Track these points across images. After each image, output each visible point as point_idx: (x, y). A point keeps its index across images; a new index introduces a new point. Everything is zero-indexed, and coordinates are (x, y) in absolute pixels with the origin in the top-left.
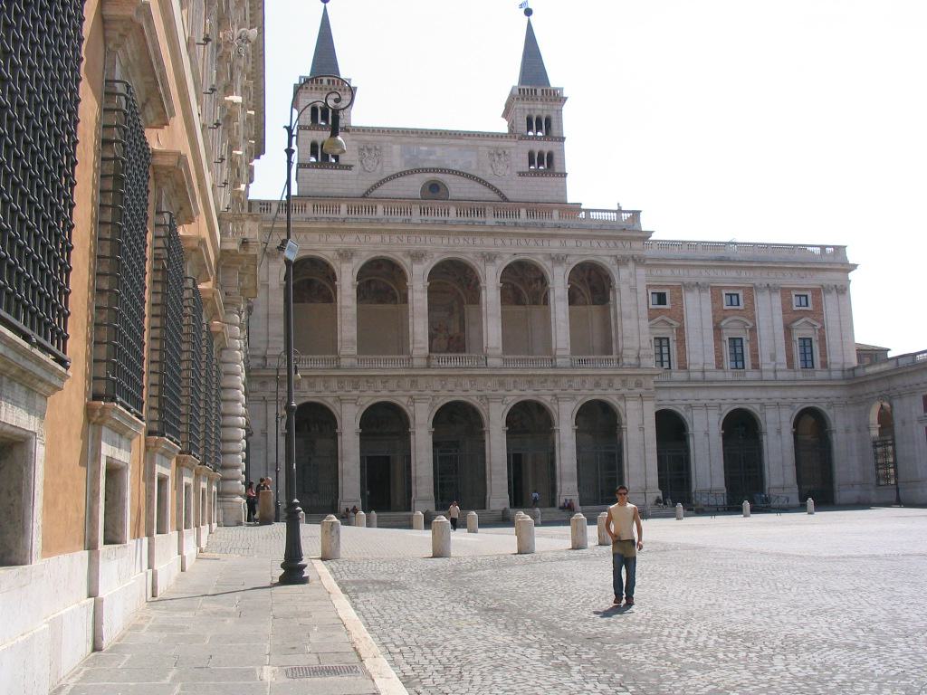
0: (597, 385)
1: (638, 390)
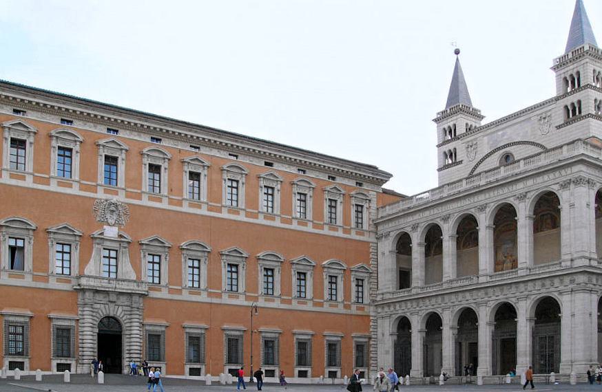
1: (571, 286)
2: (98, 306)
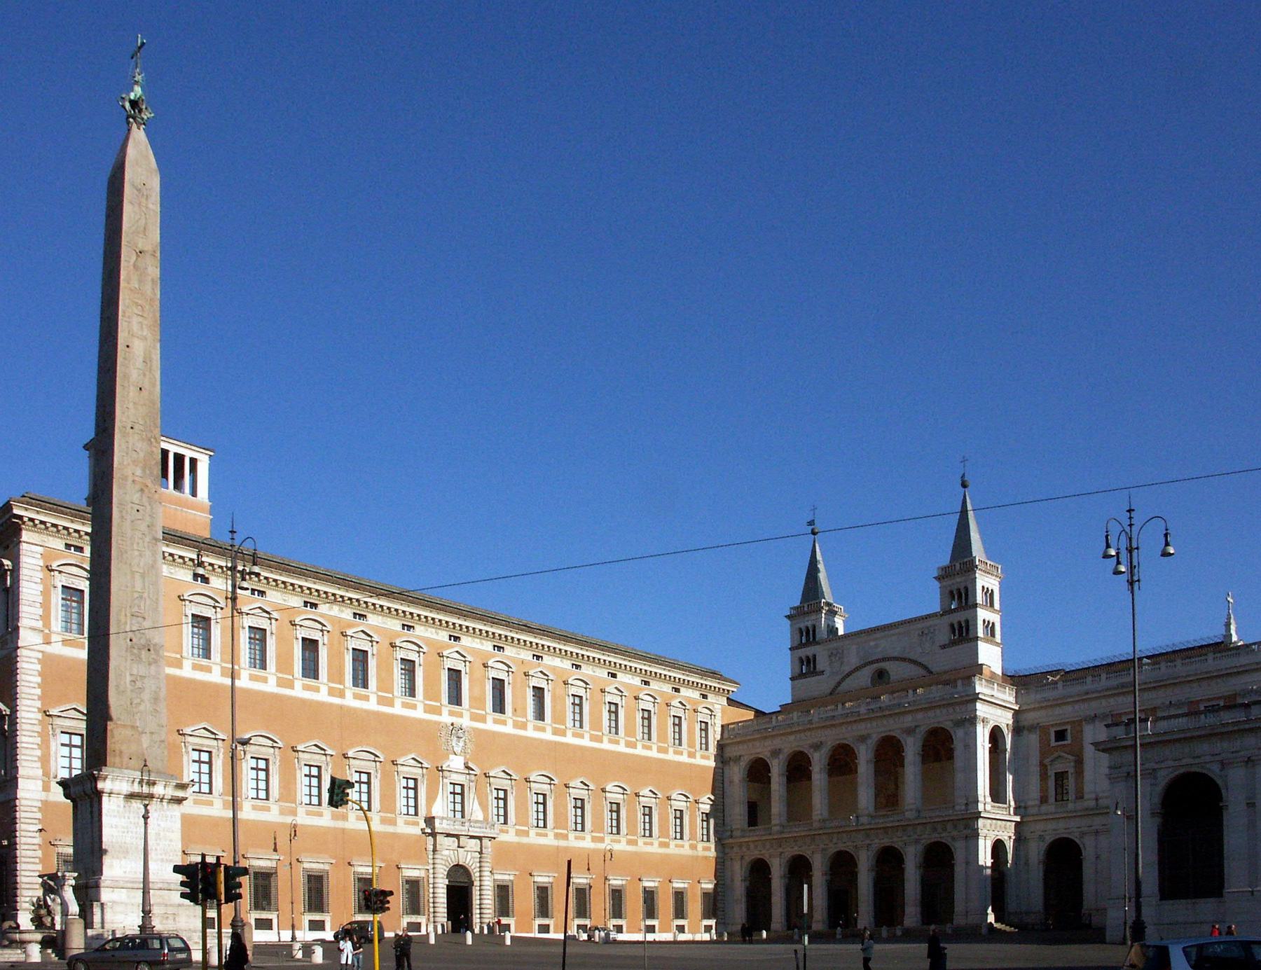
0: (935, 830)
2: (446, 852)
